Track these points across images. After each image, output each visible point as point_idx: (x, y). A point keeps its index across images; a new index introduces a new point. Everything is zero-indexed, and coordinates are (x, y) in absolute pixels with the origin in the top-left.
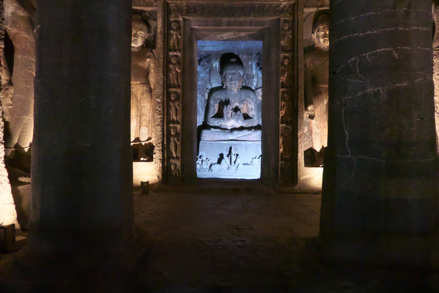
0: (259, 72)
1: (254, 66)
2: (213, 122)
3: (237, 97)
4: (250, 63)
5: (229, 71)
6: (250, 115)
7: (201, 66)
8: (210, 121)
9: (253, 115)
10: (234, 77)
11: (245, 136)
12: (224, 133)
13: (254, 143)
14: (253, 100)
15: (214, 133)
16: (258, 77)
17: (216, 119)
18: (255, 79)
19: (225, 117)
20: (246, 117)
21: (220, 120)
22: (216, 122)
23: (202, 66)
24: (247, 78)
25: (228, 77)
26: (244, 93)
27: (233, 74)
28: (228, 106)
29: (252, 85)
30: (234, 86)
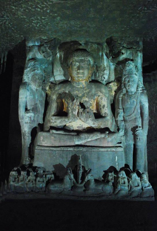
0: (112, 64)
1: (105, 57)
2: (55, 122)
3: (86, 90)
4: (100, 54)
5: (76, 58)
6: (101, 114)
7: (41, 52)
8: (51, 121)
9: (105, 113)
10: (82, 64)
11: (96, 140)
12: (69, 137)
13: (109, 149)
14: (105, 95)
15: (56, 135)
16: (110, 70)
18: (107, 72)
19: (70, 114)
20: (98, 116)
21: (63, 119)
23: (43, 52)
25: (75, 65)
27: (82, 61)
28: (75, 101)
29: (103, 79)
30: (82, 76)
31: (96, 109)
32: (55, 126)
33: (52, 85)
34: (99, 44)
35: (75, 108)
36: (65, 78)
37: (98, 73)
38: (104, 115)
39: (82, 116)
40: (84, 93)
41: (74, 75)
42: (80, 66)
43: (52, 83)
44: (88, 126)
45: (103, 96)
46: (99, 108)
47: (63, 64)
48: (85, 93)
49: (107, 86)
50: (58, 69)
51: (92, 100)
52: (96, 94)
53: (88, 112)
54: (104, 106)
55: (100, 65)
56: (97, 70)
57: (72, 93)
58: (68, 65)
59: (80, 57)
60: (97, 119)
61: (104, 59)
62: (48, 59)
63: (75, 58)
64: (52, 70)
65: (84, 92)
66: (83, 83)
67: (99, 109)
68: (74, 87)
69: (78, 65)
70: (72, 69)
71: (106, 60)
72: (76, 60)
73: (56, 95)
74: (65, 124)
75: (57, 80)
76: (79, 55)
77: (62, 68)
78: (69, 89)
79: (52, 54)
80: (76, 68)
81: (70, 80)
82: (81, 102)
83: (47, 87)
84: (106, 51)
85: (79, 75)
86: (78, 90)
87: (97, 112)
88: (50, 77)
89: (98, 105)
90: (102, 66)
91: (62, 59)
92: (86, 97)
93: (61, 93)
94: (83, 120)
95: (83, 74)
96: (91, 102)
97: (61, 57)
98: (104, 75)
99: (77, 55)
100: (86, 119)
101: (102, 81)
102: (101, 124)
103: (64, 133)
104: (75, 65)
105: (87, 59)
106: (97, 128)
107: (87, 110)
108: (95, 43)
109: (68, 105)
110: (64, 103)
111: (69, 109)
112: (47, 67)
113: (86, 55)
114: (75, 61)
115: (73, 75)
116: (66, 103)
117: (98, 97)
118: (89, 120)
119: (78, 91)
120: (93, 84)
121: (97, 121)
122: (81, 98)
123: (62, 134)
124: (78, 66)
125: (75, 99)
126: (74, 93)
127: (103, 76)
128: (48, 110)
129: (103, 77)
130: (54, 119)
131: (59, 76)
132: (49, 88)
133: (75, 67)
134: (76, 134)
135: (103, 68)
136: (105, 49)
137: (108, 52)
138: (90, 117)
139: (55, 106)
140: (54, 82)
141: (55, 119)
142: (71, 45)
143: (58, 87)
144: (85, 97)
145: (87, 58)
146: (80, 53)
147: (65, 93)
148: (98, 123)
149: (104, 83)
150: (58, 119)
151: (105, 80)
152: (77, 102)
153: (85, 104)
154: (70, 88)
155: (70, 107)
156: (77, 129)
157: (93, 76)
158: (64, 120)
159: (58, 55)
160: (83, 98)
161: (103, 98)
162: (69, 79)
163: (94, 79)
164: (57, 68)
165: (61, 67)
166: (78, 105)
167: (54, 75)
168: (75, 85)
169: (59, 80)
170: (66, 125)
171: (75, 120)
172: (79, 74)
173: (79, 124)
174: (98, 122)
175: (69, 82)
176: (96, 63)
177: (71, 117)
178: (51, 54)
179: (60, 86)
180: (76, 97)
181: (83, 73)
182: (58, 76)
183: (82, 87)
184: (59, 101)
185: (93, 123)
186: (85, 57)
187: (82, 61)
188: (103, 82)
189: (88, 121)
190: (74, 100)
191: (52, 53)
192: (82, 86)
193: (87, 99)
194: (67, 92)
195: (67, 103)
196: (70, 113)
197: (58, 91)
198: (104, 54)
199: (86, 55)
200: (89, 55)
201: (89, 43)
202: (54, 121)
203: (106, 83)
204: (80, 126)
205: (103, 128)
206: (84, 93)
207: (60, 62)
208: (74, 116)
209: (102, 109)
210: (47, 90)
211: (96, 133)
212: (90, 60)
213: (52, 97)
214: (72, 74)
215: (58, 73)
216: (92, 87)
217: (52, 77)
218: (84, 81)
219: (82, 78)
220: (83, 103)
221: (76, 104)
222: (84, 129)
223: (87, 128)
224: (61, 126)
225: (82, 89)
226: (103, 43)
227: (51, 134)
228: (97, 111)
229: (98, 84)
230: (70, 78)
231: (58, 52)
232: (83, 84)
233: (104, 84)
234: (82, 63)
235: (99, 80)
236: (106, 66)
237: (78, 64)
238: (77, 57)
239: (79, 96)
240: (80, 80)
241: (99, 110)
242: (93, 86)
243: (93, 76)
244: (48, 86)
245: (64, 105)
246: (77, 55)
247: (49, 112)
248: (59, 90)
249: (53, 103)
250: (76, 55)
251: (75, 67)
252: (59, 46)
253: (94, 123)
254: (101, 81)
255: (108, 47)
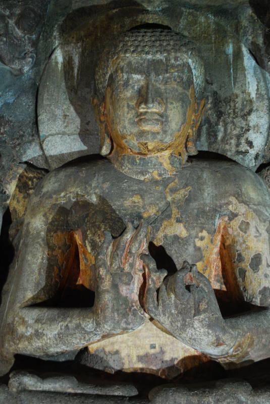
1: (249, 62)
2: (38, 335)
3: (174, 191)
5: (131, 57)
6: (247, 296)
8: (21, 329)
10: (157, 81)
17: (54, 312)
19: (107, 299)
21: (74, 319)
22: (52, 332)
24: (220, 114)
25: (126, 84)
26: (206, 174)
27: (155, 67)
28: (128, 236)
29: (244, 147)
30: (157, 128)
31: (220, 273)
32: (38, 354)
33: (31, 175)
34: (220, 12)
35: (127, 268)
36: (85, 148)
37: (221, 123)
38: (257, 301)
39: (160, 307)
40: (168, 205)
41: (125, 127)
42: (150, 86)
43: (30, 165)
44: (187, 355)
45: (251, 214)
46: (233, 269)
47: (76, 93)
48: (173, 202)
49: (260, 175)
50: (59, 112)
51: (205, 233)
52: (221, 207)
53: (188, 288)
54: (256, 261)
55: (228, 95)
56: (220, 114)
57: (115, 204)
58: (96, 91)
59: (147, 53)
60: (233, 320)
61: (244, 69)
62: (16, 66)
63: (127, 55)
64: (33, 115)
65: (169, 199)
66: (163, 162)
67: (234, 273)
68: (121, 178)
69: (142, 83)
70: (113, 104)
71: (255, 73)
72: (130, 63)
73: (45, 215)
74: (81, 346)
75: (51, 156)
76: (142, 44)
77: (72, 109)
78: (102, 188)
79: (31, 49)
80: (131, 99)
81: (105, 151)
82: (157, 243)
83: (9, 183)
84: (250, 38)
85: (146, 127)
86: (140, 190)
87: (224, 288)
88: (20, 142)
89: (229, 256)
90: (237, 96)
91: (76, 71)
92: (178, 221)
93: (68, 208)
94: (167, 325)
95: (162, 123)
96: (199, 243)
97: (68, 63)
98: (248, 130)
99: (136, 43)
100: (180, 318)
101: (241, 156)
102: (251, 345)
103: (79, 392)
104: (126, 84)
105: (176, 59)
106: (234, 360)
107: (184, 277)
108: (209, 8)
109: (96, 259)
110: (81, 250)
111: (102, 272)
112: (11, 101)
113: (172, 43)
114: (125, 69)
115: (119, 128)
116: (89, 249)
117: (230, 219)
118: (196, 324)
119: (142, 197)
120: (204, 164)
121: (233, 328)
122: (155, 223)
123: (70, 394)
124: (142, 87)
125: (130, 226)
126: (122, 205)
127: (246, 136)
128: (9, 279)
129: (243, 141)
130: (31, 322)
131: (60, 138)
132: (17, 186)
133: (129, 93)
134: (134, 392)
135: (243, 104)
136: (245, 33)
137: (260, 41)
138: (198, 312)
139: (40, 261)
140: (41, 164)
141: (38, 321)
142: (111, 19)
143: (53, 179)
144: (173, 221)
145: (179, 55)
146: (148, 37)
147: (87, 205)
148: (236, 338)
149: (250, 162)
150: (52, 320)
151: (253, 152)
152: (136, 244)
153: (172, 252)
154: (106, 185)
155: (104, 264)
156: (140, 365)
157: (203, 138)
158: (78, 326)
159: (59, 56)
160: (165, 223)
161: (253, 224)
162: (101, 148)
163: (205, 149)
164: (52, 107)
165: (72, 102)
166: (142, 256)
167: (41, 134)
168: (126, 169)
169: (63, 155)
170: (86, 349)
171: (127, 323)
172: (146, 120)
173: (147, 342)
174: (234, 333)
175: (100, 162)
176: (214, 87)
177: (108, 313)
178: (29, 48)
179: (62, 174)
180: (133, 222)
181: (161, 116)
182: (58, 139)
183: (159, 178)
184: (58, 239)
185: (212, 338)
186: (168, 52)
187: (155, 67)
188: (243, 159)
189: (190, 331)
190: (123, 231)
191: (35, 44)
192: (160, 175)
193: (181, 230)
194: (94, 199)
195: (94, 246)
196: (108, 291)
197: (54, 196)
198: (245, 50)
199: (172, 43)
200: (185, 45)
201: (183, 9)
202: (30, 331)
203: (258, 164)
204: (153, 351)
205: (257, 360)
206: (168, 205)
207: (66, 83)
208: (124, 308)
209: (249, 273)
210: (8, 197)
211: (228, 388)
212: (192, 67)
213: (28, 224)
214: (113, 123)
215: (58, 126)
216: (199, 178)
217: (30, 142)
218: (167, 153)
219: (155, 136)
220: (166, 247)
221: (134, 251)
222: (171, 368)
223: (184, 360)
224: (62, 353)
225: (161, 188)
226: (236, 9)
227: (11, 394)
228: (225, 284)
229: (225, 165)
230: (108, 141)
231: (59, 44)
232: (161, 164)
233: (248, 169)
234: (157, 75)
235: (229, 155)
236: (253, 95)
237: (139, 81)
238: (133, 51)
239: (145, 215)
240: (150, 148)
241: (236, 279)
242: (206, 175)
243: (203, 138)
244: (14, 178)
245: (81, 256)
246: (136, 43)
247: (12, 287)
248: (58, 192)
249: (30, 249)
250: (129, 44)
251: (129, 93)
252: (61, 20)
253: (218, 339)
254: (234, 158)
255: (259, 24)
